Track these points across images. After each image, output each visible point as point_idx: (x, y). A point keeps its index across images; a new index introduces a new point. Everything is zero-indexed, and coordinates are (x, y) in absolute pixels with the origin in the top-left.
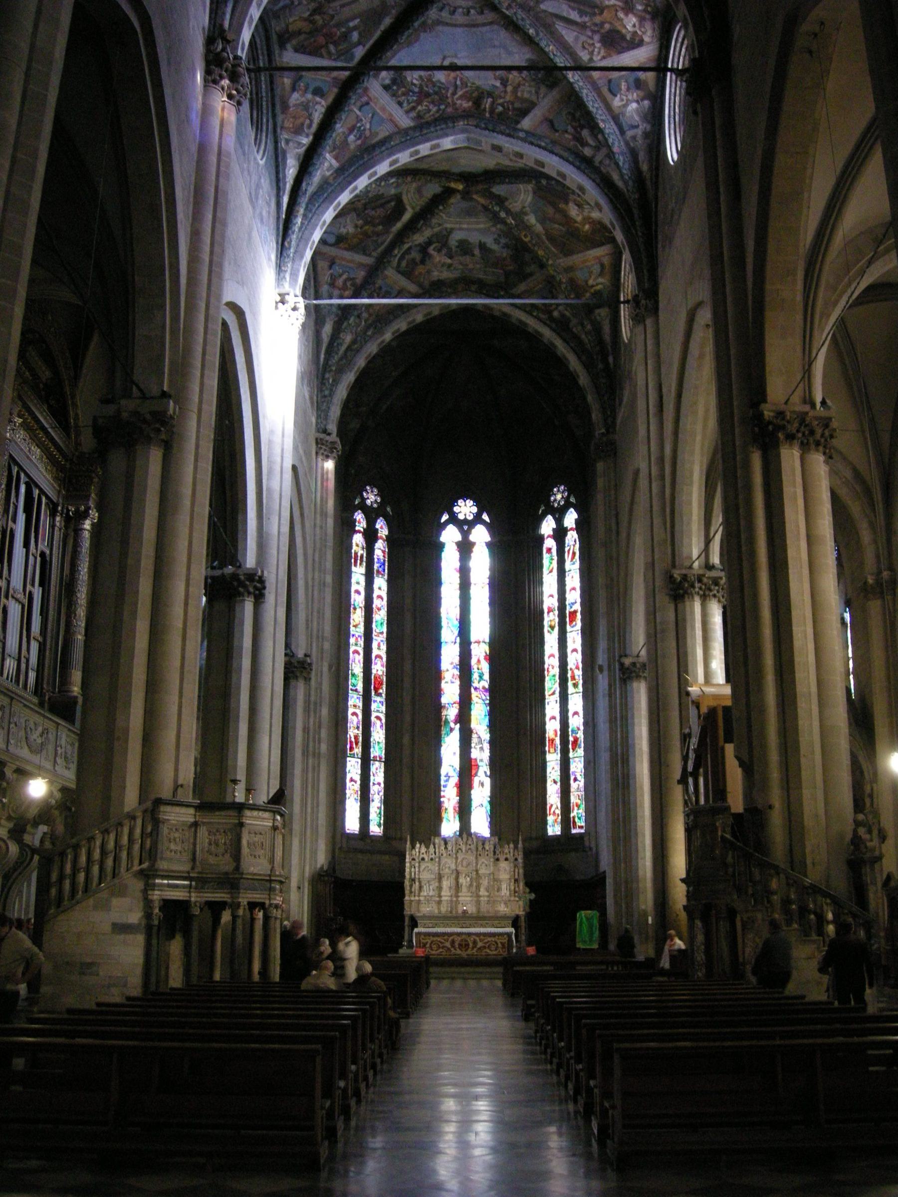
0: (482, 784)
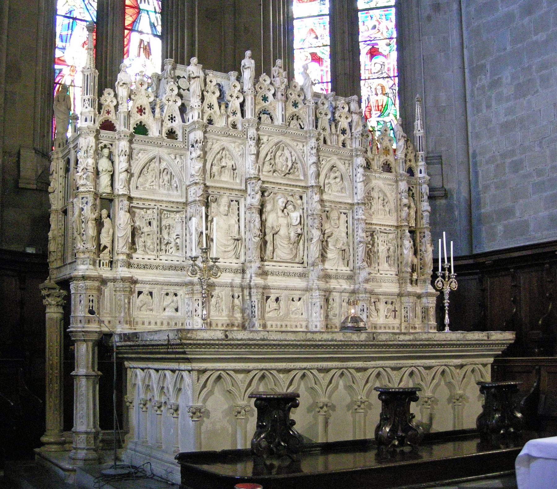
0: (147, 50)
